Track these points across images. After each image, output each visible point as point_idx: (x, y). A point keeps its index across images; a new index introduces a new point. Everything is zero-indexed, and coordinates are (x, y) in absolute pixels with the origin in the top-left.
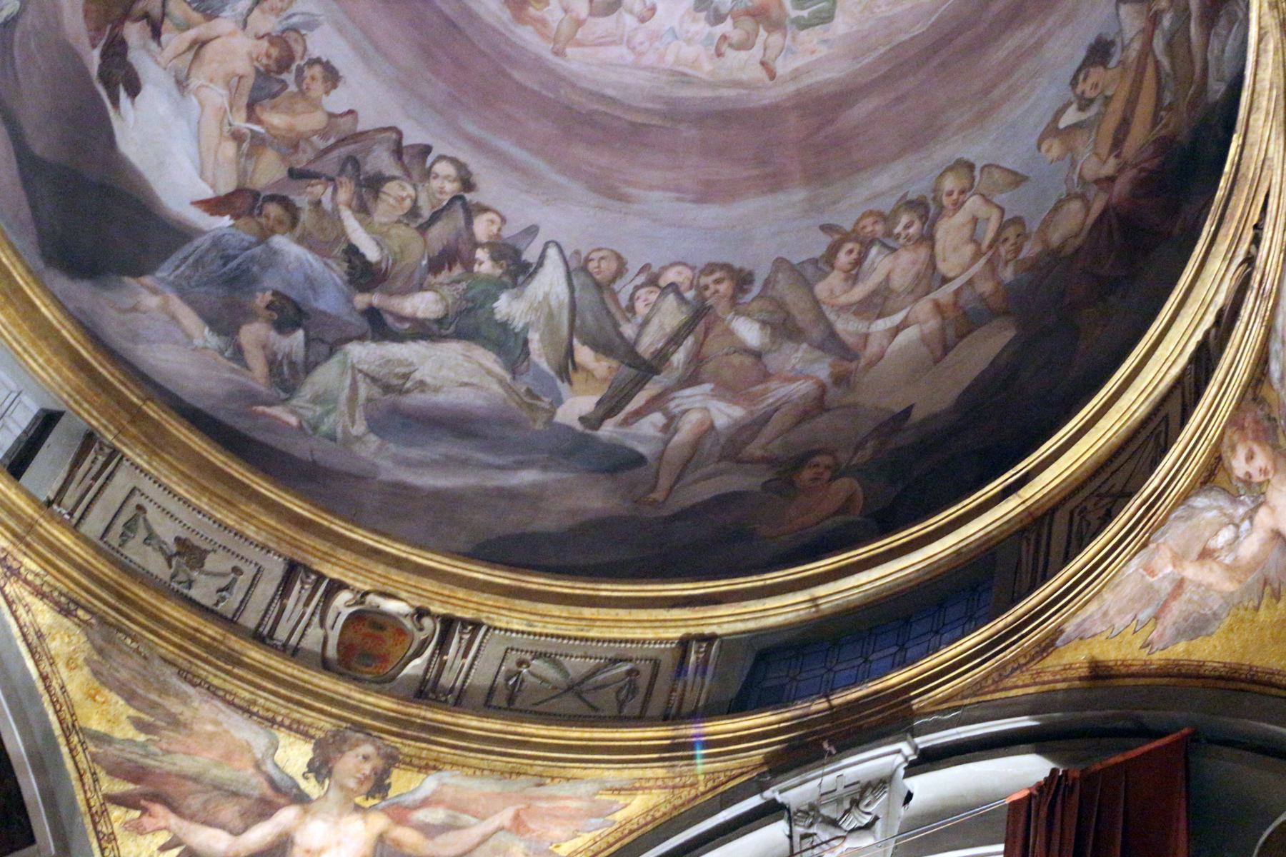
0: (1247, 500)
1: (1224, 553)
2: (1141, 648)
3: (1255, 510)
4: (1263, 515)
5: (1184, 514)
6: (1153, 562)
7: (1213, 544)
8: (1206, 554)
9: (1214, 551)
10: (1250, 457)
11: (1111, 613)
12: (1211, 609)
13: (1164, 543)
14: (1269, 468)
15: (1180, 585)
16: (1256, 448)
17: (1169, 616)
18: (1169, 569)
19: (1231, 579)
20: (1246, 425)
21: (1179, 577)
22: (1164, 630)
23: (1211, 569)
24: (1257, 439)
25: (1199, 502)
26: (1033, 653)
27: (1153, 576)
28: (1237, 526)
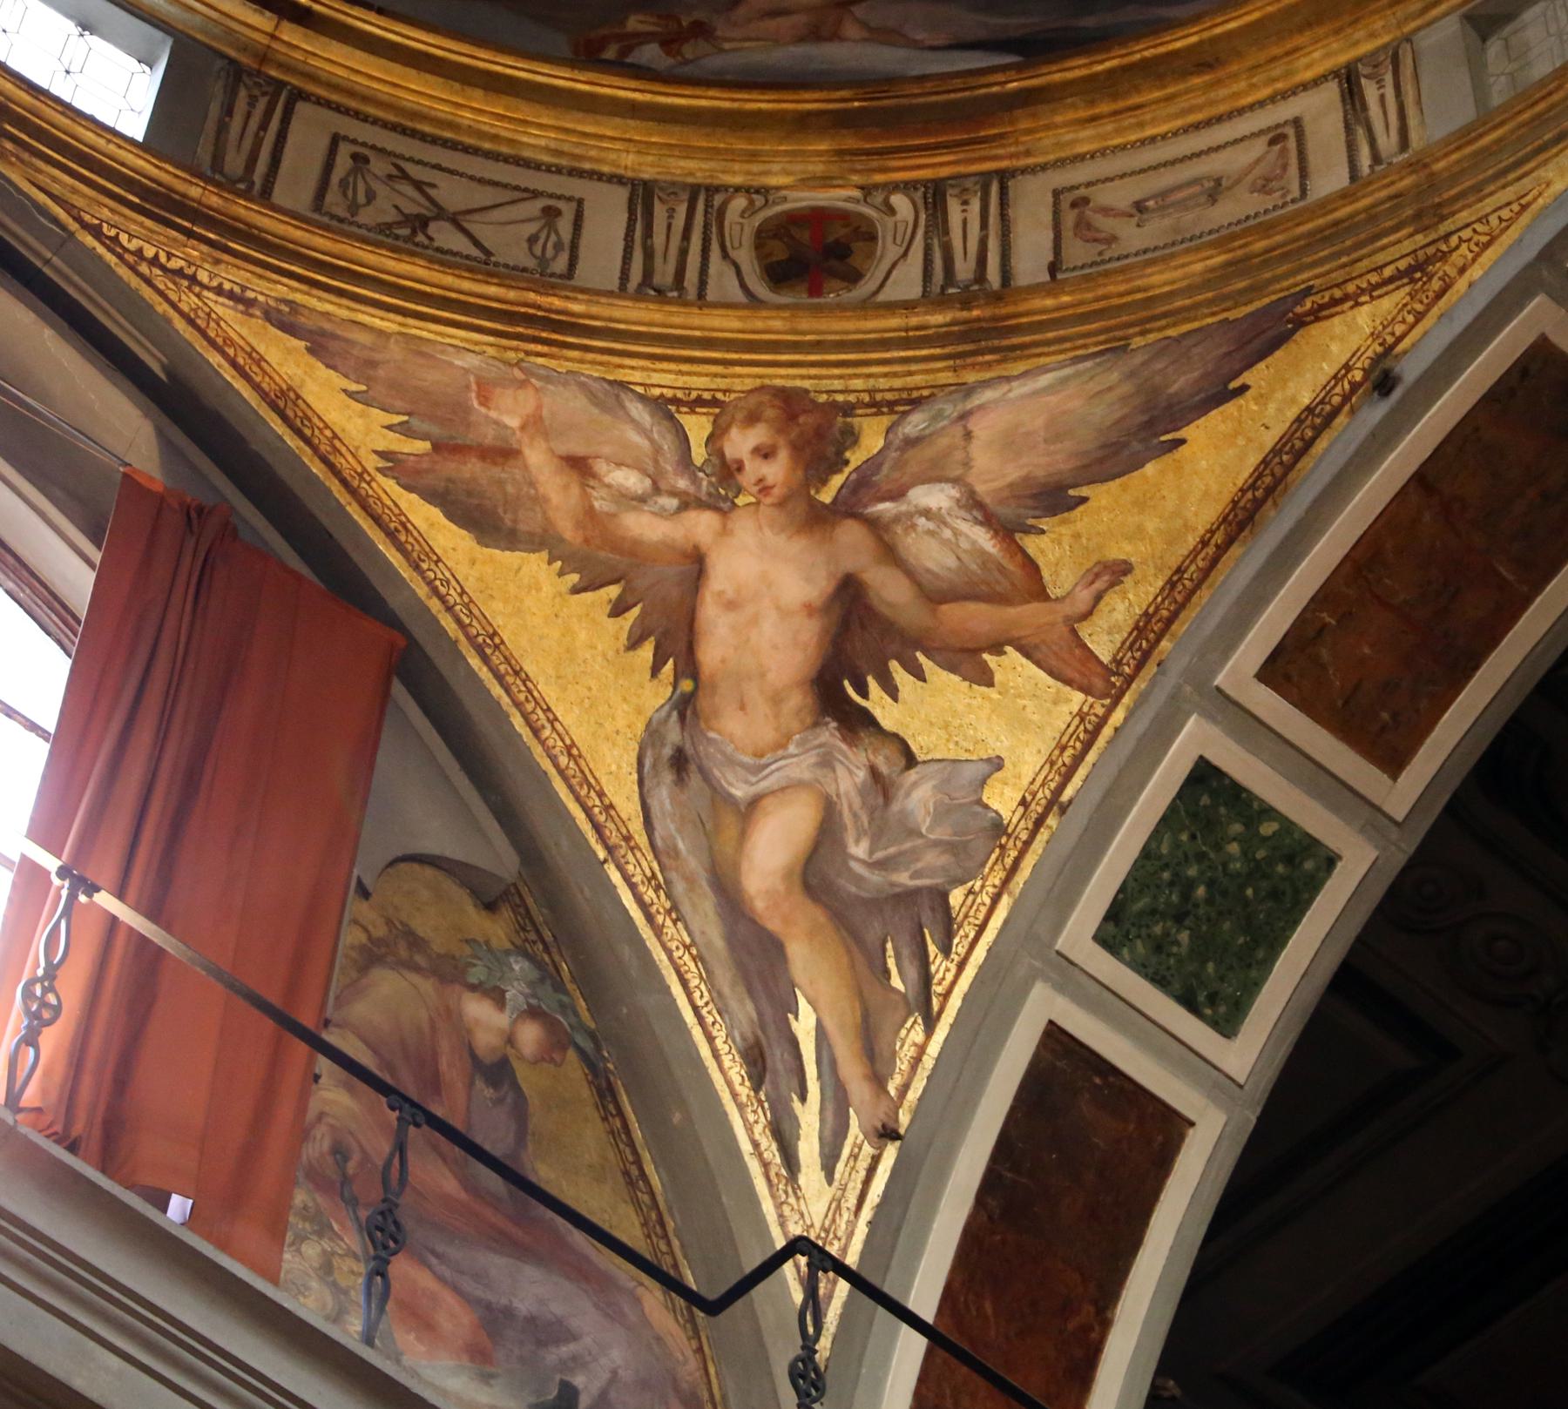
0: (705, 483)
1: (603, 492)
2: (375, 452)
3: (701, 505)
4: (702, 525)
5: (600, 395)
6: (498, 390)
7: (601, 467)
8: (579, 465)
9: (594, 476)
10: (764, 453)
11: (381, 372)
12: (515, 521)
13: (537, 390)
14: (776, 491)
15: (504, 453)
16: (783, 456)
17: (453, 465)
18: (513, 422)
19: (579, 525)
20: (802, 420)
21: (515, 446)
22: (427, 471)
23: (566, 487)
24: (796, 448)
25: (637, 410)
26: (227, 286)
27: (481, 404)
28: (657, 489)
